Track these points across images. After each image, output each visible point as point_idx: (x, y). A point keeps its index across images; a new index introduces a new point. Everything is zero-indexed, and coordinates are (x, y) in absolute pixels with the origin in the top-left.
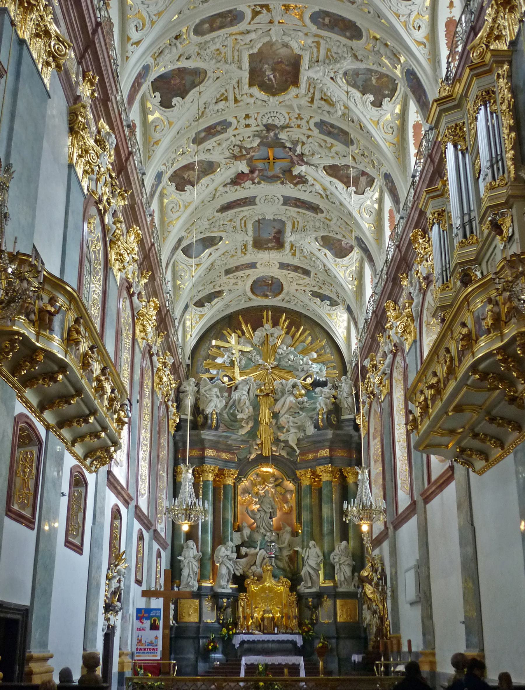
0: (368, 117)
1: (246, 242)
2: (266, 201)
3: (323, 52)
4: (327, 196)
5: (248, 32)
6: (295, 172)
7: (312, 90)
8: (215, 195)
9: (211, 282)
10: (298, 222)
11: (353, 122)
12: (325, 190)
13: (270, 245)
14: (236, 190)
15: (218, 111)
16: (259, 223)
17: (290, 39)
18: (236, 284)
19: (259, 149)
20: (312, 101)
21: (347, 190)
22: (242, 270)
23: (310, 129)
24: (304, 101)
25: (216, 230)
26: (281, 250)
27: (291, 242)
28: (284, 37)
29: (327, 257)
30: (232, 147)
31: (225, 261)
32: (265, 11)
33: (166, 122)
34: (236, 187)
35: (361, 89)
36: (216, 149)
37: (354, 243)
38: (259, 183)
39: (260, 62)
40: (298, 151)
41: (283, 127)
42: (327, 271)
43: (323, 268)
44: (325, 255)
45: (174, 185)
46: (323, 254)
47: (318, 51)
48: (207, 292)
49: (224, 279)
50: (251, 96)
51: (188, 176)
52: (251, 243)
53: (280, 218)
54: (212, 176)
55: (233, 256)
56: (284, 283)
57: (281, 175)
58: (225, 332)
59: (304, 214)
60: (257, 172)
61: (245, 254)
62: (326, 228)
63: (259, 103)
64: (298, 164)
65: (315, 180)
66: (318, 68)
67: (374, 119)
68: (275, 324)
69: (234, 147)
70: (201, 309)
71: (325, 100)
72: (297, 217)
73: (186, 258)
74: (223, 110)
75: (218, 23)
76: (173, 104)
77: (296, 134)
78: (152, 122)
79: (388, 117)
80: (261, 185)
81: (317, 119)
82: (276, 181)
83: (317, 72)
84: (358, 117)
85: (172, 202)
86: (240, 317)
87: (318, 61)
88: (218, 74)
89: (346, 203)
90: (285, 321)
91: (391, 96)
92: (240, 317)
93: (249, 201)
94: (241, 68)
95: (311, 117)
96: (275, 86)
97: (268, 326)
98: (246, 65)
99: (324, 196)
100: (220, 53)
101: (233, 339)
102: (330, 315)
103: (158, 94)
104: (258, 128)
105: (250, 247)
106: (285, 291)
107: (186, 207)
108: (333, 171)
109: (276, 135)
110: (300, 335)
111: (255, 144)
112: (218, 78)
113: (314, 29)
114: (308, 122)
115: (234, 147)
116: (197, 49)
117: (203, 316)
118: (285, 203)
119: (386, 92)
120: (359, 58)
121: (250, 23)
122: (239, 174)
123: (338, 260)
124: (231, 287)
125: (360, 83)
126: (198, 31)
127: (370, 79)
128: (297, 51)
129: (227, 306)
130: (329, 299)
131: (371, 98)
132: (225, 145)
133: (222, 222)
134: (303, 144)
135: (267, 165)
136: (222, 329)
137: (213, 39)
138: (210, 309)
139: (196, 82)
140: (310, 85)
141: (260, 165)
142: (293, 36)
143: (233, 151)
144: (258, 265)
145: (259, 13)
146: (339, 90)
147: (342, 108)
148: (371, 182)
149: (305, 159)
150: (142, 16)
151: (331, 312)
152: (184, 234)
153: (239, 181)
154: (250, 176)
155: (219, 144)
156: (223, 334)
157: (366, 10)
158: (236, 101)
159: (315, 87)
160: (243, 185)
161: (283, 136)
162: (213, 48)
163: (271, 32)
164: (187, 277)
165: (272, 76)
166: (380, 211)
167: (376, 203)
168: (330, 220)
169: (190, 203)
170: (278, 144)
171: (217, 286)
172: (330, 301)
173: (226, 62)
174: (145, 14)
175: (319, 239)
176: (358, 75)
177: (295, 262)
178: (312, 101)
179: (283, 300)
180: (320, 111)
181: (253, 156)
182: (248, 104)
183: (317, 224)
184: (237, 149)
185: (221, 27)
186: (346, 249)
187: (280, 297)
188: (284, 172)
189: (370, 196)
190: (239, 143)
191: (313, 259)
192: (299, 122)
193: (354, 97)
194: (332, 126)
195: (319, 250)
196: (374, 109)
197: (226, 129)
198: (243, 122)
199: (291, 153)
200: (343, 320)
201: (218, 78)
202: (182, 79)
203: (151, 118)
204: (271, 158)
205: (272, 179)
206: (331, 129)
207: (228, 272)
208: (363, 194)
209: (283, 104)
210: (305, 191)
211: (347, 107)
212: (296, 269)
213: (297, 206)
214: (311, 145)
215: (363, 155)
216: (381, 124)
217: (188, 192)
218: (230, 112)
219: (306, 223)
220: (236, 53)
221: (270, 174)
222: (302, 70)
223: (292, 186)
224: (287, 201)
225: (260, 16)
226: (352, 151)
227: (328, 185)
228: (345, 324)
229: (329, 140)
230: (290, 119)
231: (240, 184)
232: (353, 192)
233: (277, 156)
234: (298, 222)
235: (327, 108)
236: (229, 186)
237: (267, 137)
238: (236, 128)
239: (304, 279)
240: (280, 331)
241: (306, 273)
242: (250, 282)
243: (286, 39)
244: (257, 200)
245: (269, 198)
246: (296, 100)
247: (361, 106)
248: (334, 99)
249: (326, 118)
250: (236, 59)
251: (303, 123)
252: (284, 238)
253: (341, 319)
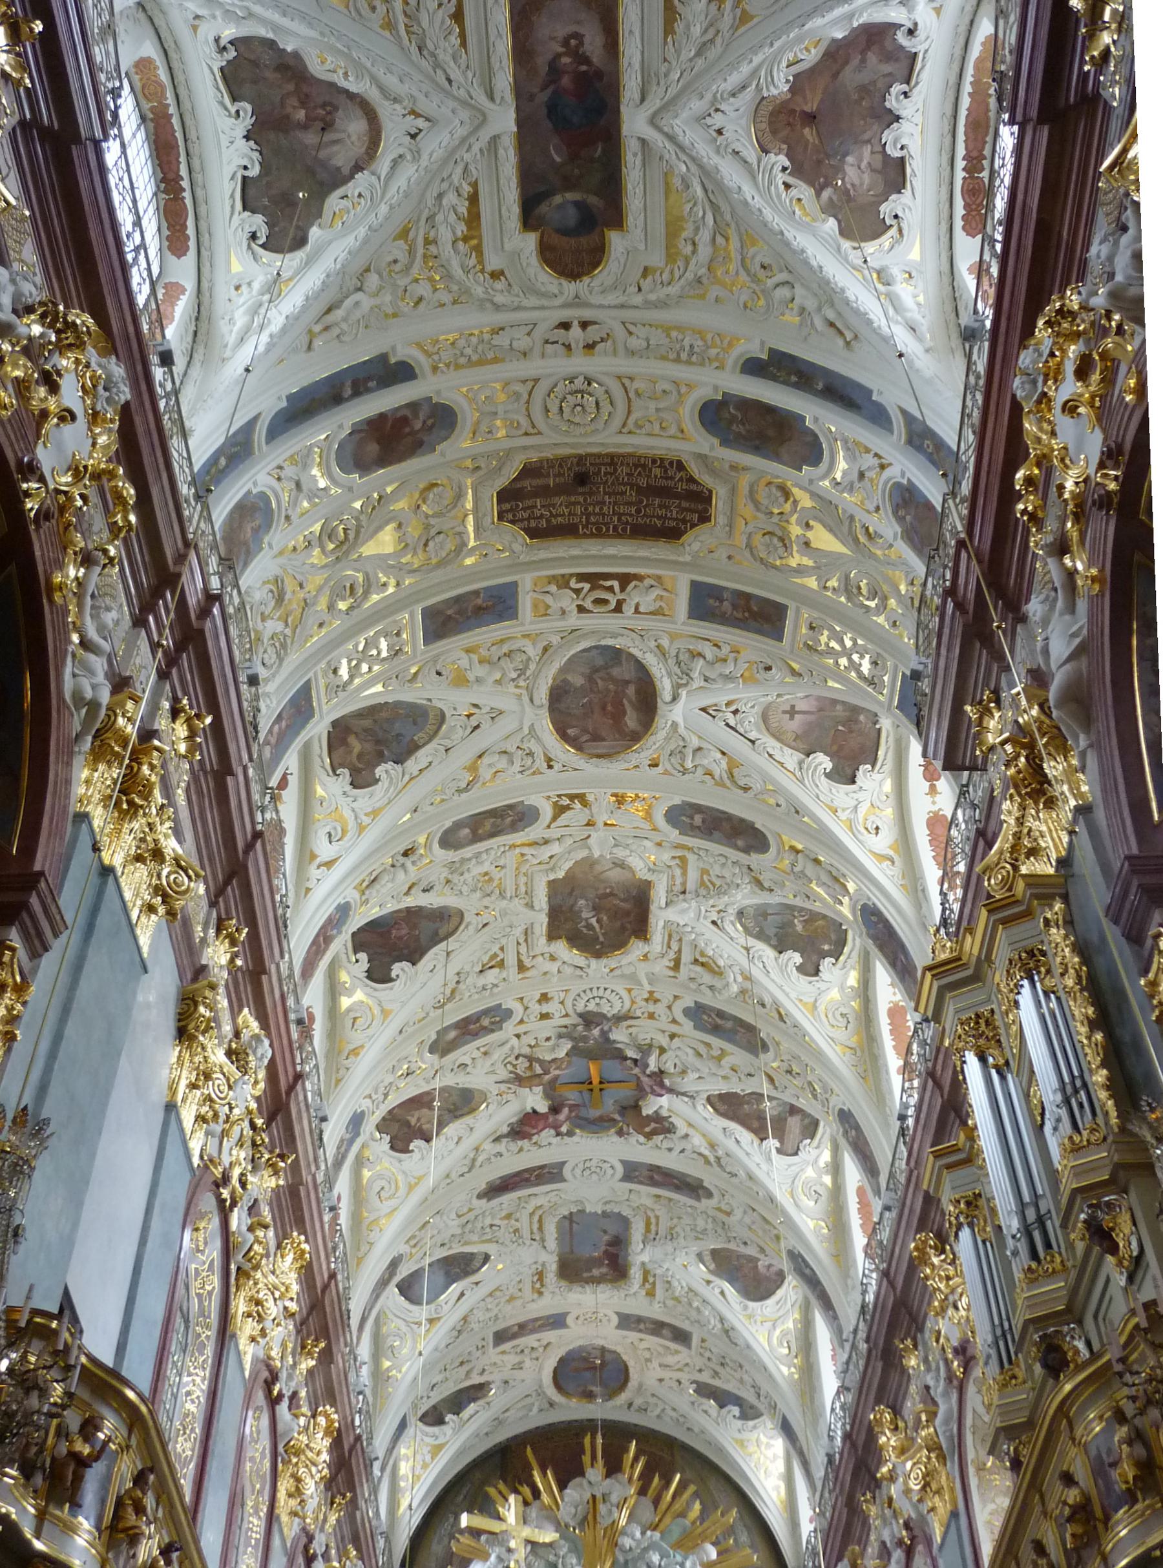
0: (793, 995)
1: (543, 1265)
2: (587, 1173)
4: (718, 1159)
5: (546, 842)
6: (648, 1110)
7: (675, 946)
8: (474, 1160)
9: (462, 1363)
10: (657, 1218)
11: (763, 1005)
12: (712, 1146)
13: (596, 1272)
14: (521, 1150)
15: (484, 989)
16: (573, 1224)
17: (628, 852)
18: (519, 1366)
19: (569, 1064)
20: (676, 966)
21: (760, 1145)
22: (533, 1331)
23: (674, 1021)
24: (661, 967)
25: (475, 1238)
26: (622, 1283)
27: (643, 1264)
28: (615, 850)
29: (725, 1298)
30: (512, 1059)
31: (496, 1311)
33: (376, 1011)
34: (520, 1143)
35: (774, 942)
36: (479, 1062)
37: (785, 1265)
38: (570, 1134)
39: (571, 894)
40: (653, 1066)
41: (619, 1019)
42: (728, 1332)
43: (719, 1326)
44: (722, 1293)
45: (387, 1138)
46: (717, 1291)
47: (684, 873)
48: (450, 1388)
49: (493, 1354)
50: (553, 958)
51: (419, 1119)
52: (554, 1267)
53: (616, 1210)
54: (468, 1120)
55: (512, 1299)
56: (631, 1364)
57: (617, 1117)
58: (491, 1491)
59: (670, 1200)
60: (566, 1110)
61: (540, 1293)
62: (720, 1230)
63: (568, 970)
64: (653, 1092)
65: (690, 1125)
66: (686, 905)
67: (805, 1000)
68: (613, 1468)
69: (517, 1058)
70: (435, 1430)
71: (703, 964)
72: (656, 1207)
73: (406, 1304)
74: (496, 986)
75: (488, 825)
76: (393, 974)
77: (646, 1031)
78: (349, 1010)
79: (835, 994)
80: (575, 1139)
81: (688, 1001)
82: (608, 1129)
83: (683, 911)
84: (772, 995)
85: (380, 1176)
86: (529, 1449)
87: (684, 892)
89: (760, 1175)
90: (636, 1459)
91: (837, 954)
92: (529, 1449)
93: (548, 1174)
95: (676, 997)
96: (601, 939)
97: (595, 1473)
98: (542, 899)
99: (712, 1159)
100: (491, 880)
101: (511, 1510)
102: (742, 1443)
103: (363, 956)
104: (566, 1021)
105: (551, 1277)
106: (633, 1384)
107: (411, 1188)
108: (730, 1106)
109: (604, 1034)
110: (674, 1497)
111: (561, 1053)
112: (485, 925)
113: (674, 834)
114: (669, 1007)
115: (517, 1058)
116: (445, 873)
117: (439, 1447)
118: (627, 1177)
119: (826, 947)
120: (766, 885)
122: (527, 1114)
123: (751, 1304)
124: (506, 1374)
125: (771, 931)
126: (448, 840)
127: (792, 925)
128: (643, 874)
129: (498, 1422)
130: (738, 1401)
131: (797, 958)
132: (498, 1055)
133: (488, 1221)
134: (662, 1050)
135: (586, 1095)
136: (485, 1482)
137: (477, 856)
138: (457, 1431)
139: (442, 932)
140: (670, 936)
141: (572, 1096)
142: (634, 847)
143: (515, 1066)
144: (570, 1320)
145: (567, 808)
146: (731, 946)
147: (740, 979)
148: (811, 1128)
149: (667, 1082)
150: (342, 816)
151: (745, 1435)
152: (404, 1249)
153: (527, 1129)
154: (551, 1119)
155: (485, 1053)
156: (487, 1496)
157: (772, 801)
158: (521, 967)
159: (680, 940)
160: (535, 1138)
161: (619, 1035)
162: (477, 870)
163: (591, 841)
164: (405, 1349)
165: (593, 921)
166: (837, 1190)
167: (827, 1173)
168: (728, 1214)
169: (420, 1179)
170: (608, 1051)
171: (475, 1371)
172: (740, 1406)
173: (502, 895)
174: (347, 814)
175: (707, 1258)
176: (765, 915)
177: (655, 1311)
178: (676, 966)
179: (630, 1405)
180: (693, 986)
181: (556, 1078)
182: (545, 973)
183: (701, 1223)
184: (523, 1064)
185: (493, 835)
186: (768, 1279)
187: (623, 1397)
188: (624, 1110)
189: (811, 1158)
190: (526, 1050)
191: (695, 1304)
192: (651, 1008)
193: (760, 957)
194: (721, 1014)
195: (708, 1282)
196: (804, 980)
197: (502, 1021)
198: (536, 1009)
199: (636, 1071)
200: (775, 1457)
201: (485, 925)
202: (414, 927)
203: (345, 1002)
204: (596, 1081)
205: (598, 1125)
206: (719, 1021)
207: (501, 1337)
208: (796, 1154)
209: (617, 972)
210: (670, 1150)
211: (748, 978)
212: (657, 1328)
213: (653, 1183)
214: (679, 1053)
215: (789, 1072)
216: (821, 1008)
217: (416, 1155)
218: (510, 990)
219: (675, 1221)
220: (523, 879)
221: (594, 1113)
222: (653, 908)
223: (642, 1139)
224: (632, 1172)
225: (569, 814)
226: (766, 1064)
227: (719, 1136)
228: (780, 1466)
229: (716, 1042)
230: (633, 1002)
231: (528, 1136)
232: (774, 1151)
233: (606, 1076)
234: (657, 1218)
235: (707, 978)
236: (505, 1140)
237: (585, 1039)
238: (522, 1021)
239: (677, 1352)
240: (623, 1488)
241: (681, 1337)
242: (551, 1363)
243: (620, 853)
244: (567, 1172)
245: (593, 1167)
246: (643, 964)
247: (778, 977)
248: (721, 963)
249: (707, 999)
250: (523, 889)
251: (660, 1009)
252: (627, 1255)
253: (770, 1453)
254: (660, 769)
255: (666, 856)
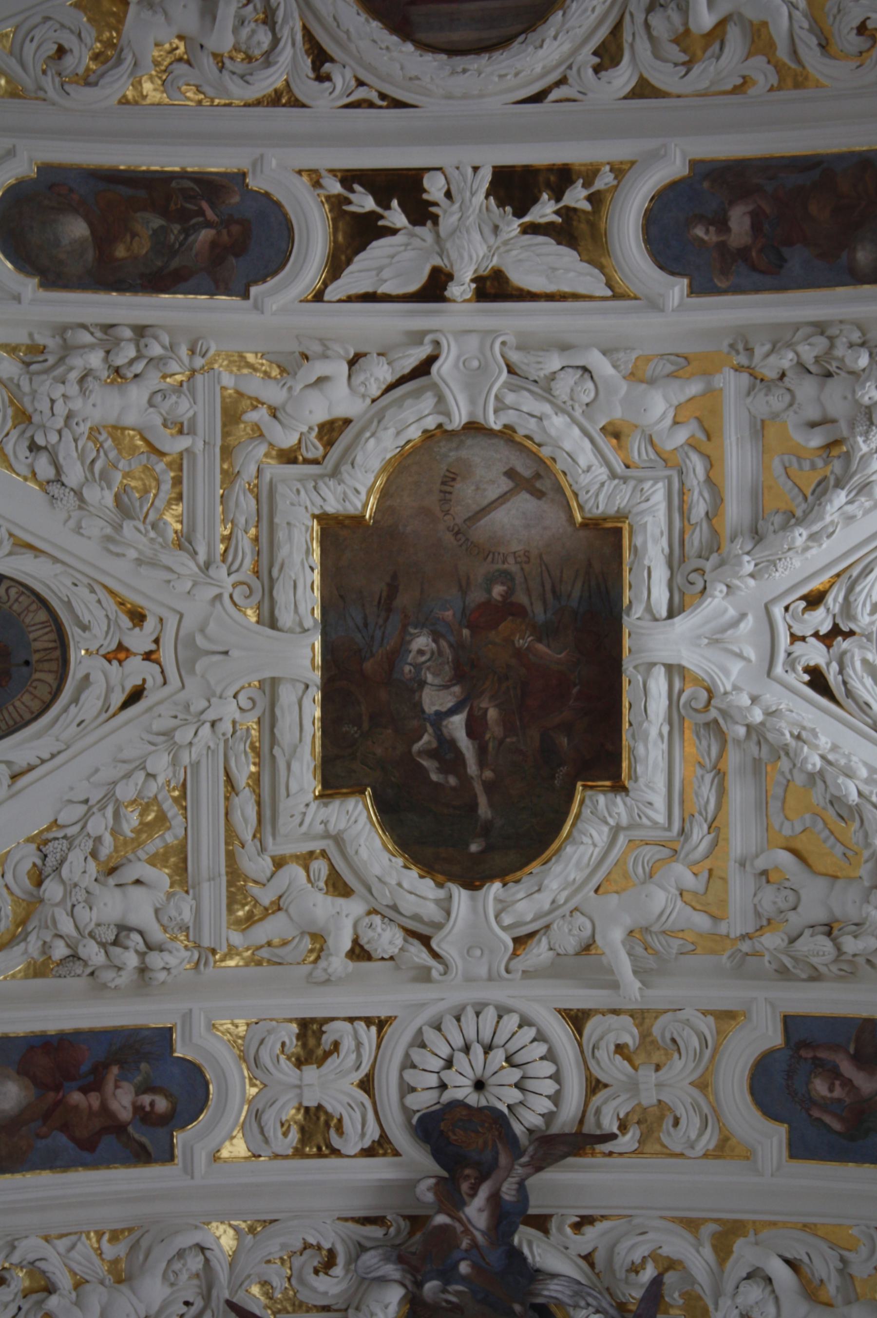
3: (738, 460)
23: (724, 1148)
32: (396, 217)
39: (387, 604)
63: (386, 939)
88: (136, 671)
94: (273, 624)
96: (484, 810)
121: (319, 297)
163: (443, 368)
165: (457, 724)
201: (135, 696)
209: (539, 953)
225: (379, 248)
254: (622, 78)
255: (658, 406)
